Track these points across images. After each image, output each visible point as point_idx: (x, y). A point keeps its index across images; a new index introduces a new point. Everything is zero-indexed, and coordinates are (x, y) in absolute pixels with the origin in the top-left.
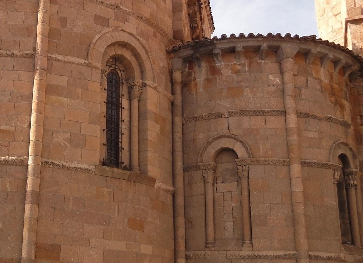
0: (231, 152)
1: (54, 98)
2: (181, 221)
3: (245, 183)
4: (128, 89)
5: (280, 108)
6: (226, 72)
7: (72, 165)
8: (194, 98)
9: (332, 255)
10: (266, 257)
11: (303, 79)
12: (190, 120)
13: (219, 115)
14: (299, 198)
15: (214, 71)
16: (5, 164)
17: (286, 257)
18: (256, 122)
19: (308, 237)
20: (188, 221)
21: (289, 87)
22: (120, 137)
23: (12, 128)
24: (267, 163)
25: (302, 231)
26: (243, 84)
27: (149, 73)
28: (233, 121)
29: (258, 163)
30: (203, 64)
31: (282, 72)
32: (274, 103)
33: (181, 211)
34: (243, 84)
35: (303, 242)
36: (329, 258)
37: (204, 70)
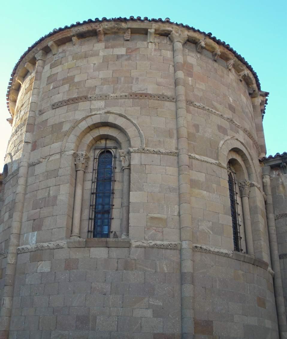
1: (196, 191)
4: (239, 188)
7: (216, 250)
8: (283, 199)
12: (282, 216)
16: (160, 248)
22: (238, 228)
23: (164, 216)
27: (254, 176)
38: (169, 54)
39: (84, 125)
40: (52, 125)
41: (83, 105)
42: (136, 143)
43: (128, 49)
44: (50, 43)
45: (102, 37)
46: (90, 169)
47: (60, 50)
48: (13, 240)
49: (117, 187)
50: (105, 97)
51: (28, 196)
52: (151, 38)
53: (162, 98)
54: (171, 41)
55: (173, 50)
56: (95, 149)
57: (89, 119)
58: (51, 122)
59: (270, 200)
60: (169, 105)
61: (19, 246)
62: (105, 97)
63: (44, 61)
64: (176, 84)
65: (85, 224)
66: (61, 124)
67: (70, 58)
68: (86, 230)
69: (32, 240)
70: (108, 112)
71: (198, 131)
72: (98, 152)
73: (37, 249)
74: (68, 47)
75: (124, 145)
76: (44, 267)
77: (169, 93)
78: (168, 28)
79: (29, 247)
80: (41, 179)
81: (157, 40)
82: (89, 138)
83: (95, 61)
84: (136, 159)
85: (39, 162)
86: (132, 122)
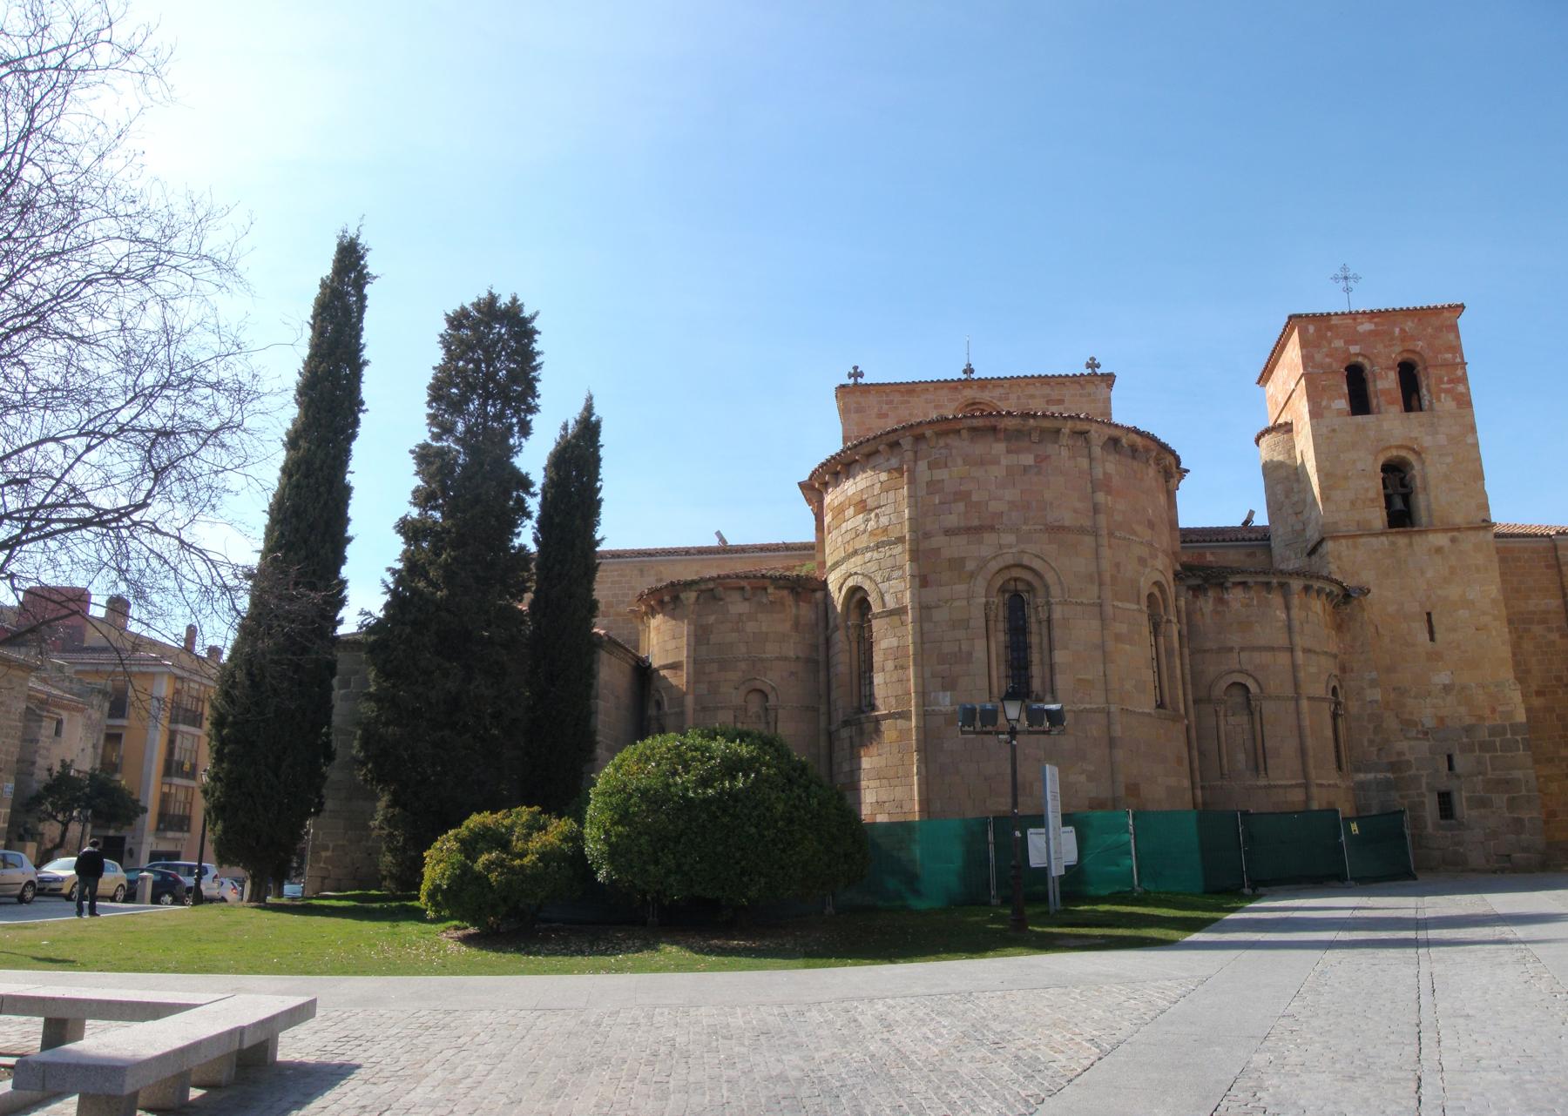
2: (1195, 753)
6: (1235, 605)
10: (1281, 786)
13: (1231, 649)
15: (1221, 601)
17: (1297, 786)
18: (1266, 657)
20: (1201, 753)
21: (1296, 624)
23: (1089, 677)
24: (1278, 698)
25: (1311, 762)
30: (1210, 594)
31: (1288, 608)
32: (1281, 639)
33: (1195, 744)
35: (1313, 773)
37: (1211, 601)
38: (1084, 463)
39: (994, 566)
41: (989, 537)
42: (1055, 590)
43: (1036, 456)
44: (928, 433)
45: (1002, 435)
46: (1001, 618)
47: (942, 443)
49: (1034, 640)
52: (1064, 440)
53: (1082, 530)
54: (1087, 441)
55: (1091, 459)
59: (1185, 632)
60: (1088, 540)
64: (1096, 509)
65: (1003, 682)
66: (962, 560)
67: (960, 461)
70: (1023, 552)
74: (953, 441)
75: (1041, 591)
77: (1087, 523)
78: (1085, 426)
81: (1070, 442)
82: (999, 582)
83: (997, 472)
84: (1057, 613)
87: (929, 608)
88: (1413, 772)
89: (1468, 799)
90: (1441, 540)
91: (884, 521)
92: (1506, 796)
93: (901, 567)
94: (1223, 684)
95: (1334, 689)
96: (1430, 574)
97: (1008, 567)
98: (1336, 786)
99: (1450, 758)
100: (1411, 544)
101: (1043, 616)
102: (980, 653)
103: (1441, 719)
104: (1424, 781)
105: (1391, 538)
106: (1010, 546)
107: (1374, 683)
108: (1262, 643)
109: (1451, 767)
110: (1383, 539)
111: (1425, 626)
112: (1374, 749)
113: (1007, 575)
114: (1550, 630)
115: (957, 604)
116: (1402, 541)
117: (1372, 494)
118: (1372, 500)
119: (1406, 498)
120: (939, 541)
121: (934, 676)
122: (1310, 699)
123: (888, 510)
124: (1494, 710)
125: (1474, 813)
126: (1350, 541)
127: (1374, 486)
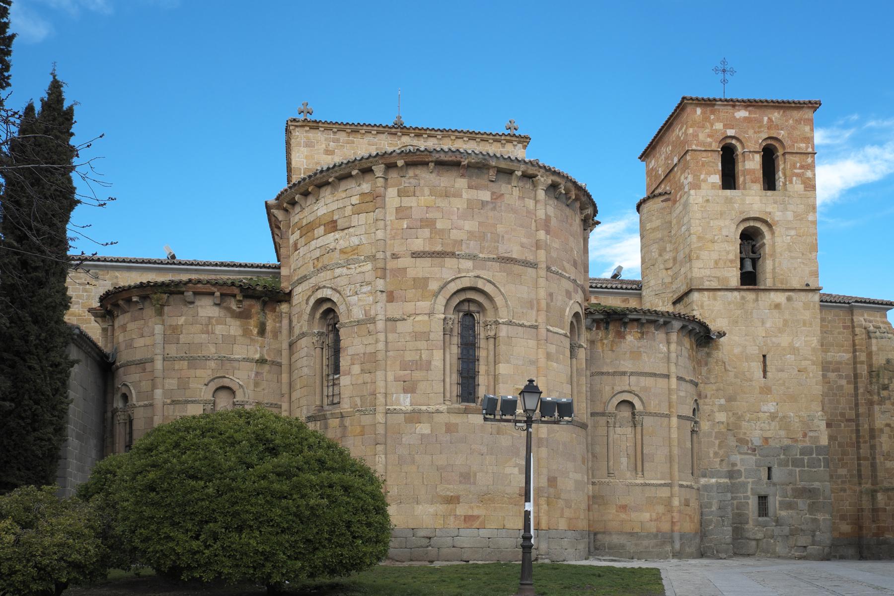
0: (631, 404)
3: (639, 428)
5: (666, 373)
9: (689, 483)
10: (653, 485)
11: (679, 348)
14: (675, 443)
19: (679, 471)
21: (673, 356)
24: (656, 415)
25: (676, 467)
26: (641, 349)
28: (633, 379)
29: (650, 414)
34: (641, 349)
36: (687, 486)
39: (453, 287)
40: (414, 279)
41: (449, 262)
46: (455, 333)
48: (381, 399)
49: (482, 354)
50: (473, 257)
51: (390, 354)
53: (526, 264)
56: (459, 311)
57: (458, 281)
58: (411, 273)
61: (386, 405)
62: (473, 257)
63: (386, 179)
66: (426, 280)
68: (455, 394)
69: (405, 402)
70: (478, 277)
71: (552, 301)
72: (461, 314)
73: (413, 411)
76: (424, 428)
77: (530, 258)
79: (403, 408)
80: (408, 338)
82: (456, 301)
84: (504, 331)
85: (404, 319)
86: (500, 291)
87: (395, 320)
88: (743, 479)
89: (780, 503)
90: (780, 298)
91: (355, 241)
92: (808, 501)
93: (368, 284)
94: (615, 401)
95: (694, 410)
96: (768, 325)
97: (464, 290)
98: (691, 487)
99: (769, 469)
100: (757, 300)
101: (492, 333)
102: (437, 362)
103: (766, 439)
104: (750, 486)
105: (743, 293)
106: (468, 271)
107: (722, 408)
108: (647, 370)
109: (769, 478)
110: (736, 294)
111: (761, 365)
112: (718, 460)
113: (462, 297)
114: (840, 377)
115: (419, 318)
116: (750, 296)
117: (731, 256)
118: (731, 261)
119: (754, 262)
120: (405, 262)
121: (396, 380)
122: (679, 417)
123: (360, 230)
124: (805, 435)
125: (783, 513)
126: (711, 293)
127: (733, 249)
